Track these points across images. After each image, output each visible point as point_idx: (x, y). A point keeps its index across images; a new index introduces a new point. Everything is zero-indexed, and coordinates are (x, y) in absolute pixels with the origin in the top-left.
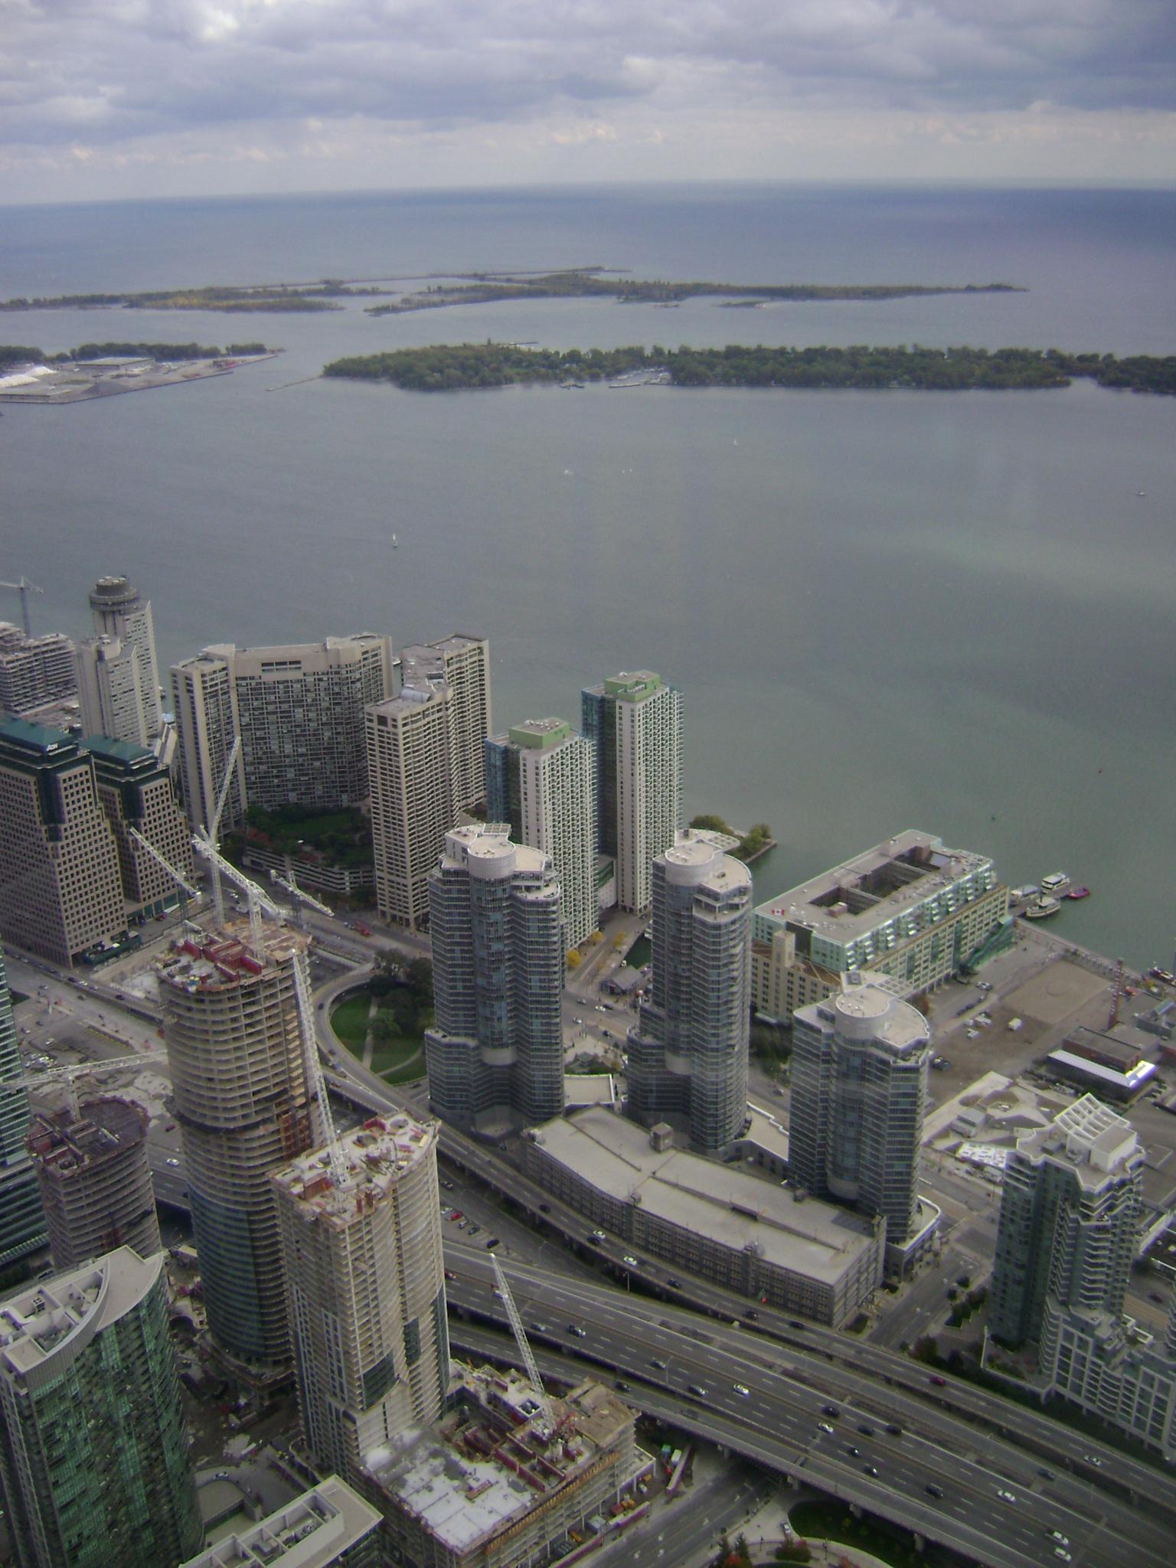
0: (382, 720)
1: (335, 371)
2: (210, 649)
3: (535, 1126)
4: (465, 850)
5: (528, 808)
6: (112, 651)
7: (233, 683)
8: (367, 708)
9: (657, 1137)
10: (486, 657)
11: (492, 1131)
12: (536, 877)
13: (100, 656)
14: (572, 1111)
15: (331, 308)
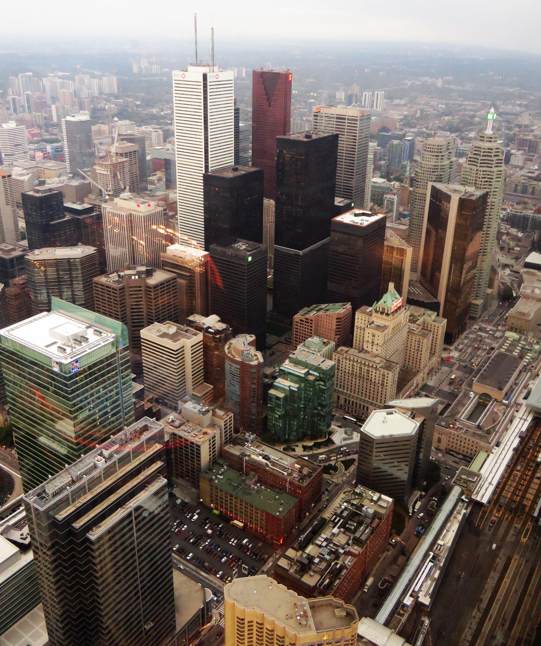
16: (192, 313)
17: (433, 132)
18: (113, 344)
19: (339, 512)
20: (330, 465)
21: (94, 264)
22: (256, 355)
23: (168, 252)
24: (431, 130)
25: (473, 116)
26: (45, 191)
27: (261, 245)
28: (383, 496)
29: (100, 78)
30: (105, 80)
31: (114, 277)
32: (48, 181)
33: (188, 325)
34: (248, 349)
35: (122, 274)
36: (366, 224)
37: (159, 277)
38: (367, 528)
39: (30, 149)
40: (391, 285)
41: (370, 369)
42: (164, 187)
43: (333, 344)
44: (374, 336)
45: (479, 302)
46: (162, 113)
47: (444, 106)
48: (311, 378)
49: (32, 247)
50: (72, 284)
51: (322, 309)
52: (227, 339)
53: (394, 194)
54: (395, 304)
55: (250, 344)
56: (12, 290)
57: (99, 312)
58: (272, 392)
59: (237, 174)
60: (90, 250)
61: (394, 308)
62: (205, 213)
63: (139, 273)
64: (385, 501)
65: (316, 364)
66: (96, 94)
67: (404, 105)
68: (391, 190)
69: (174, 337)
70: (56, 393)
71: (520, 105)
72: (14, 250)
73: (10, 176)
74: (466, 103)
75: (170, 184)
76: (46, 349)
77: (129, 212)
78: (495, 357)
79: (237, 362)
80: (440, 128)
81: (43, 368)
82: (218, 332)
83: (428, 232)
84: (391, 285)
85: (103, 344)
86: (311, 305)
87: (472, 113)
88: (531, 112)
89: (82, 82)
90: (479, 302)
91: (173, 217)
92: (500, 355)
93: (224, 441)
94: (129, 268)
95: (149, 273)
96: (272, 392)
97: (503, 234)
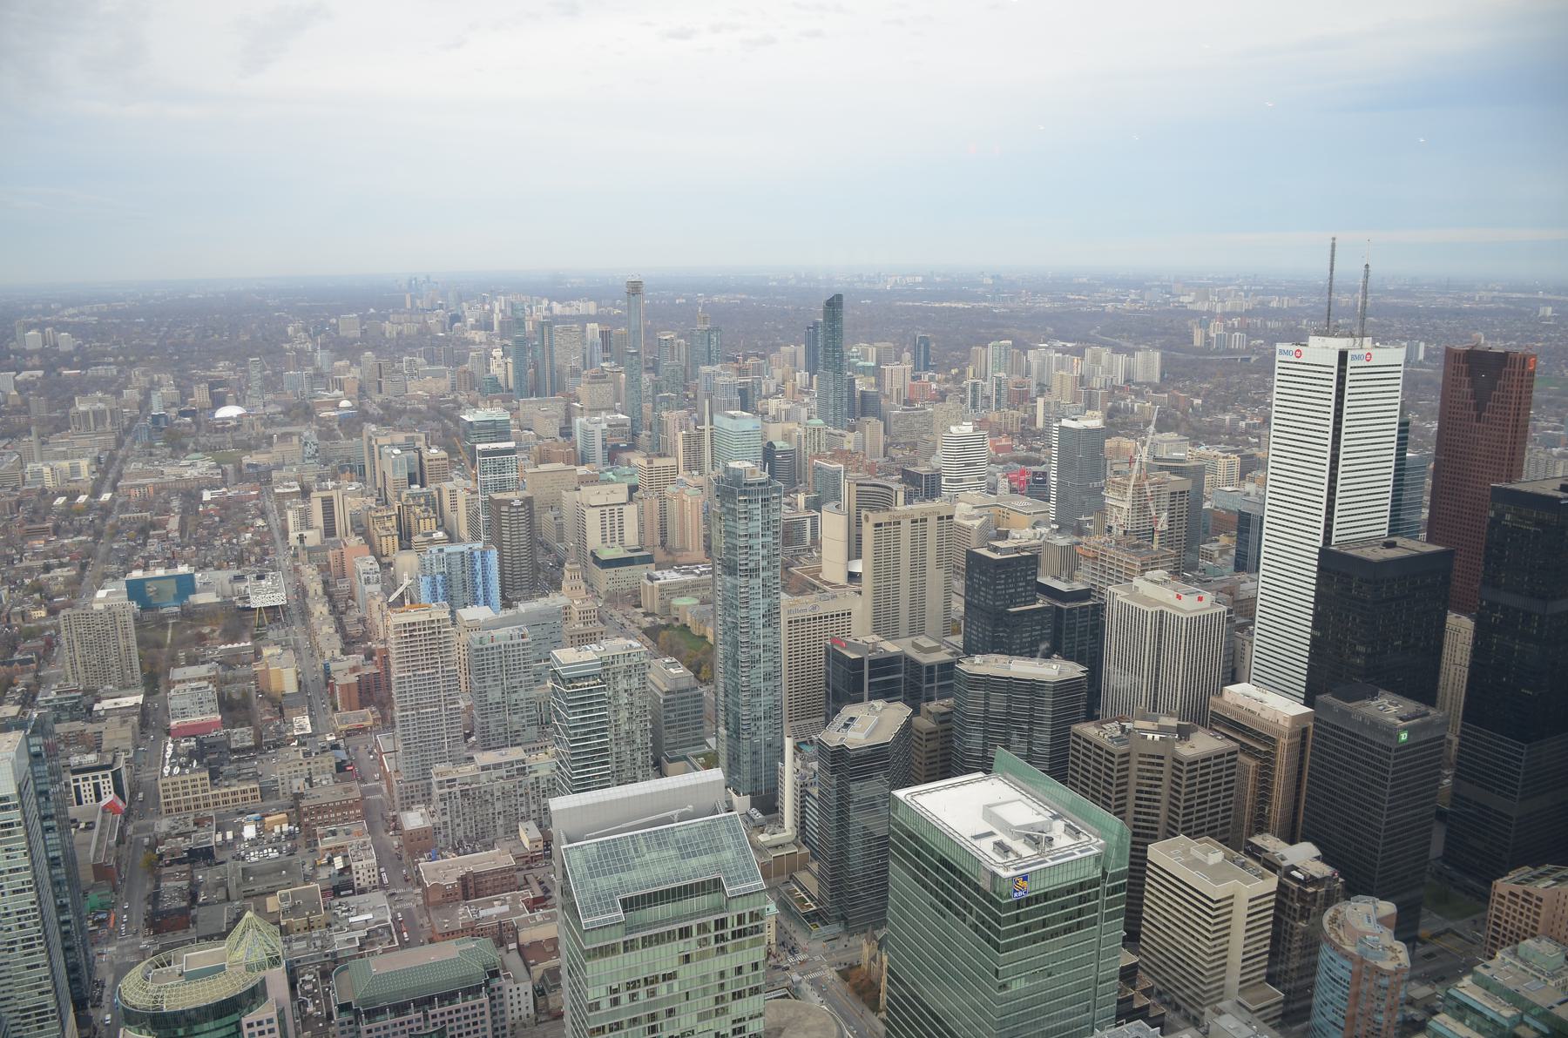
16: (1260, 831)
18: (1098, 858)
21: (1078, 699)
22: (1391, 949)
23: (1226, 697)
26: (1008, 551)
27: (1432, 712)
29: (1130, 352)
30: (1139, 355)
31: (1113, 728)
32: (1013, 533)
33: (1248, 853)
34: (1377, 931)
35: (1128, 726)
37: (1203, 744)
39: (990, 473)
42: (1232, 567)
46: (1242, 424)
49: (970, 650)
50: (1031, 730)
52: (1330, 900)
55: (1381, 921)
56: (924, 723)
57: (1084, 793)
59: (1391, 554)
60: (1074, 670)
62: (1314, 627)
63: (1161, 730)
66: (1120, 381)
69: (1215, 873)
70: (977, 929)
72: (937, 649)
73: (950, 517)
75: (1246, 561)
76: (977, 843)
77: (1158, 608)
79: (1347, 956)
81: (961, 875)
82: (1311, 880)
85: (1079, 855)
89: (1096, 359)
91: (1242, 628)
94: (1144, 719)
95: (1184, 733)
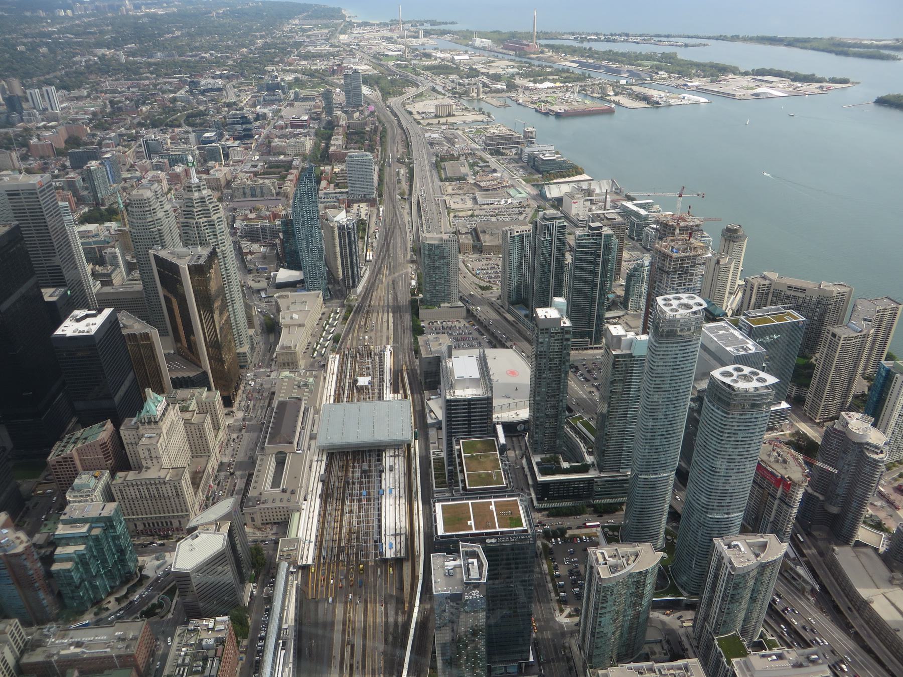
0: (834, 335)
1: (882, 102)
2: (766, 273)
3: (837, 545)
4: (847, 424)
5: (886, 411)
6: (724, 261)
7: (772, 291)
8: (828, 327)
9: (893, 578)
10: (899, 312)
11: (815, 533)
12: (877, 447)
13: (718, 262)
14: (859, 544)
15: (894, 58)
17: (134, 131)
19: (180, 661)
20: (154, 605)
22: (18, 538)
24: (130, 128)
25: (174, 100)
28: (218, 619)
36: (94, 330)
38: (213, 661)
40: (149, 392)
41: (158, 486)
43: (107, 473)
44: (149, 450)
45: (246, 349)
47: (134, 90)
48: (96, 532)
51: (78, 439)
53: (113, 247)
54: (159, 409)
58: (55, 567)
61: (159, 414)
64: (222, 622)
65: (94, 514)
67: (87, 97)
68: (108, 243)
71: (221, 76)
74: (161, 80)
78: (277, 408)
80: (140, 125)
83: (167, 300)
84: (149, 392)
86: (64, 437)
87: (171, 95)
88: (234, 82)
90: (246, 349)
92: (282, 405)
93: (18, 653)
96: (55, 567)
97: (247, 254)
